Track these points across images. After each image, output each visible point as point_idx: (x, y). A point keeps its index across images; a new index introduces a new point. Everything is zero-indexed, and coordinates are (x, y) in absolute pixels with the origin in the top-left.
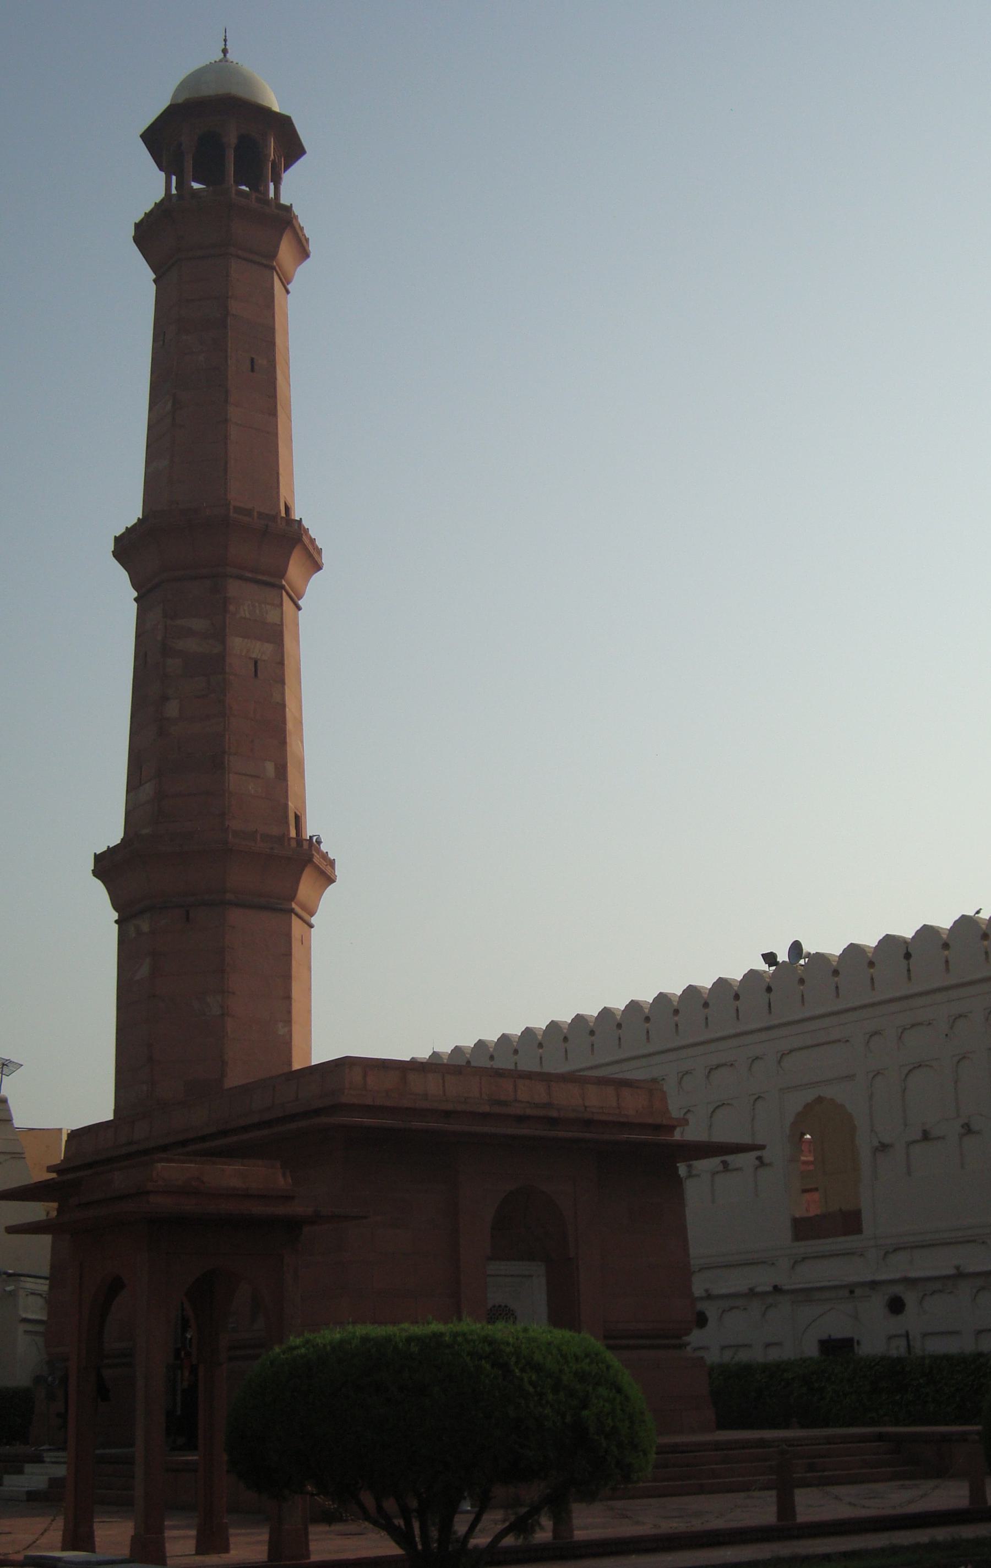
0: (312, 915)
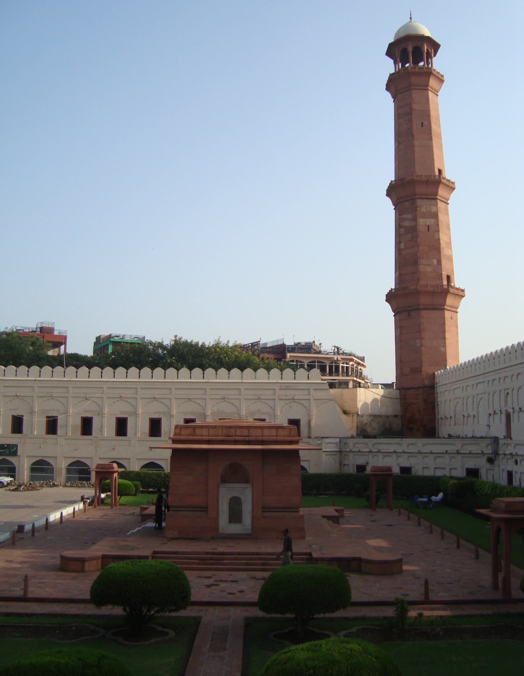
0: (457, 308)
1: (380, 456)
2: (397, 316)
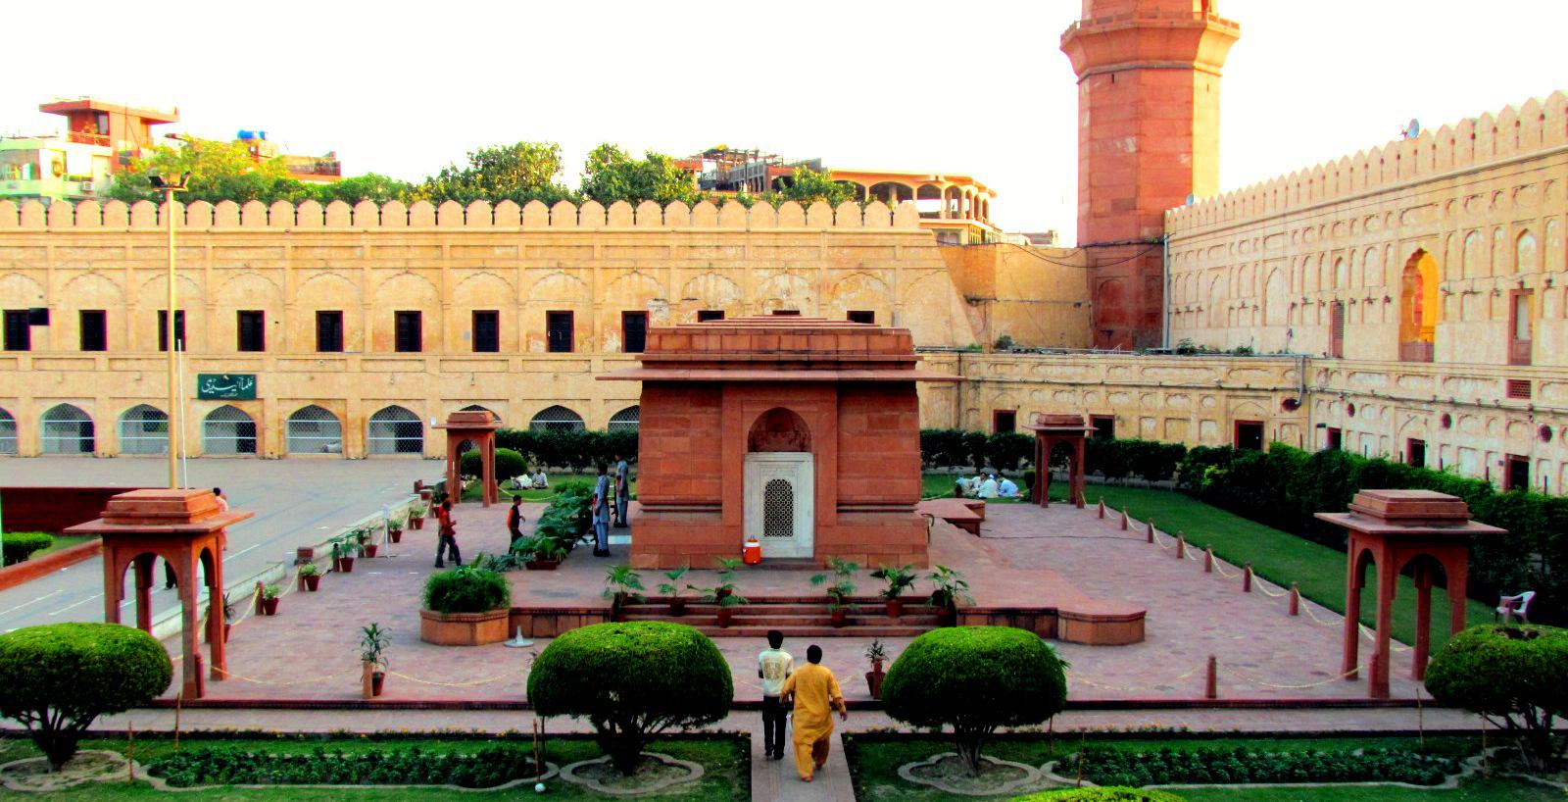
0: (1220, 66)
1: (1048, 392)
2: (1086, 85)
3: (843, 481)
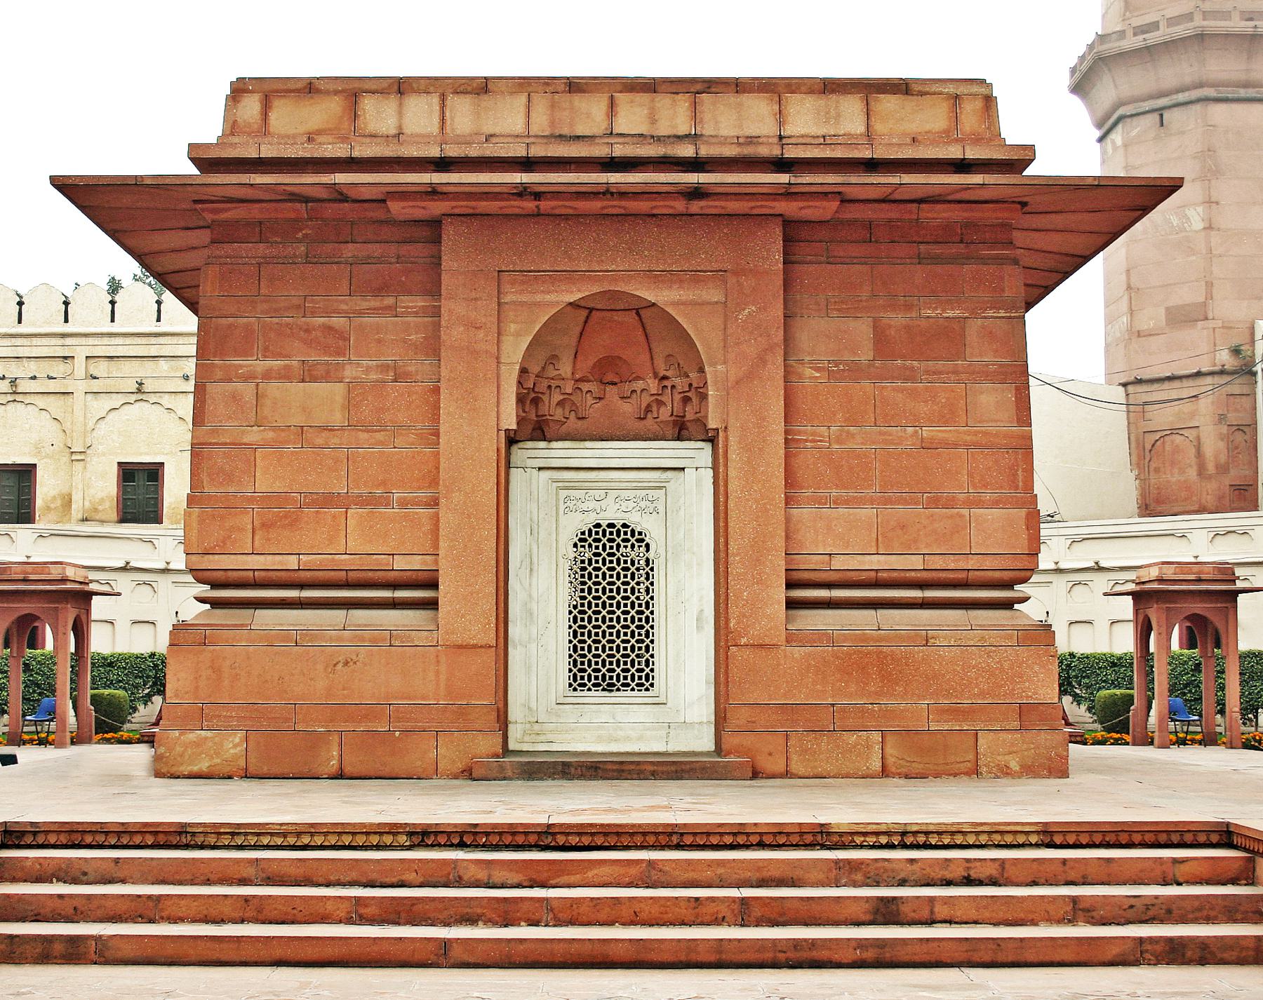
3: (802, 513)
